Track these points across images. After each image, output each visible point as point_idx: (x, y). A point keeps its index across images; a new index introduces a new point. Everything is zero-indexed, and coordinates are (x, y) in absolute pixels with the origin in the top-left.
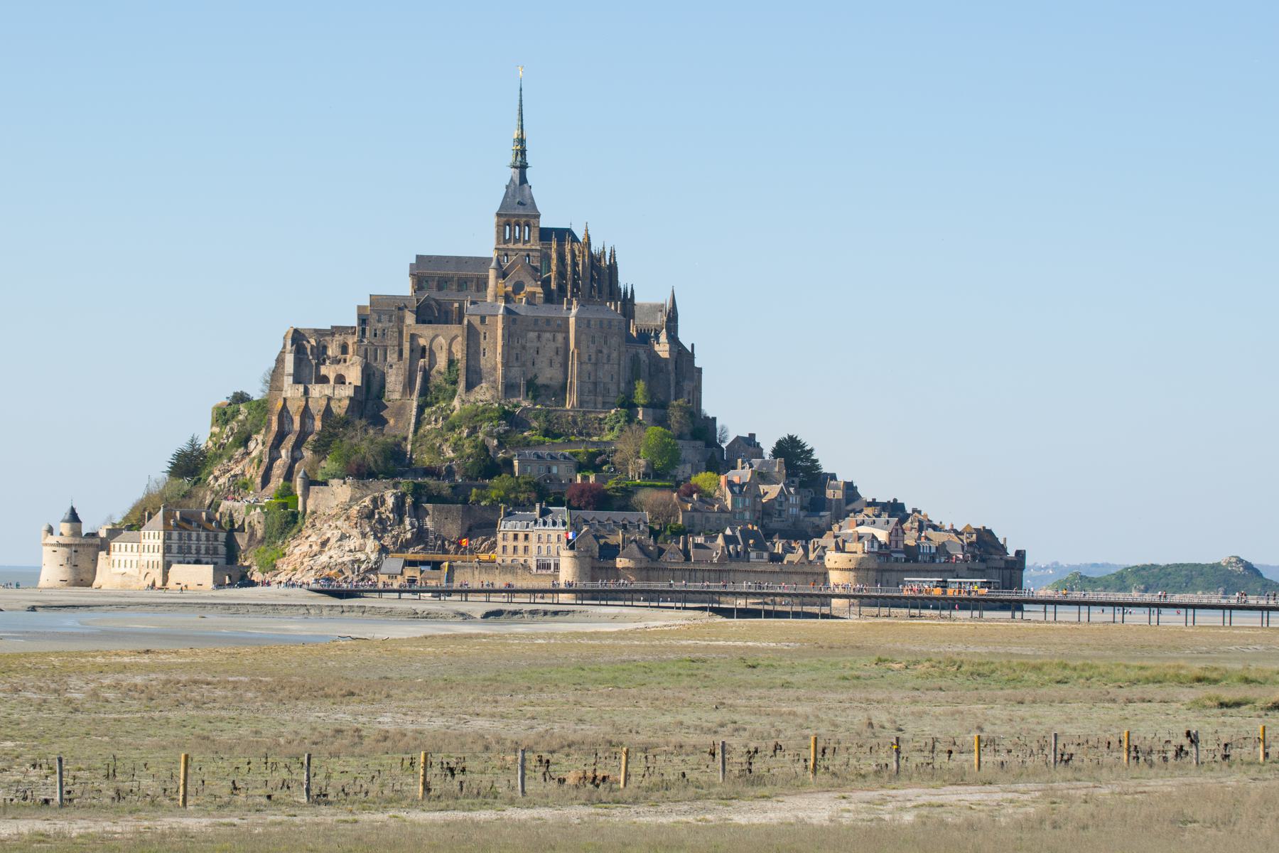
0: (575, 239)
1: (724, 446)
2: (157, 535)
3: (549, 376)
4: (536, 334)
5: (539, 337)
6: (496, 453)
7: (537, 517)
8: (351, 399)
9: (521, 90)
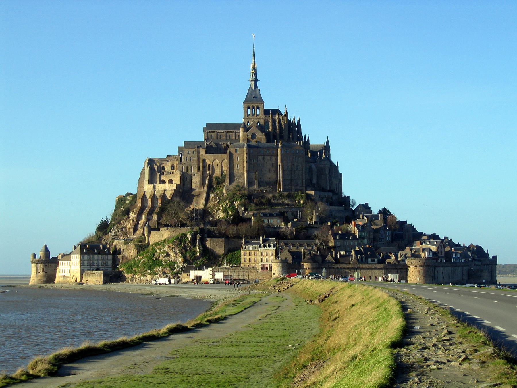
0: (281, 114)
1: (353, 209)
2: (77, 257)
3: (269, 177)
4: (262, 157)
5: (264, 158)
6: (243, 214)
7: (261, 243)
8: (175, 190)
9: (254, 45)
